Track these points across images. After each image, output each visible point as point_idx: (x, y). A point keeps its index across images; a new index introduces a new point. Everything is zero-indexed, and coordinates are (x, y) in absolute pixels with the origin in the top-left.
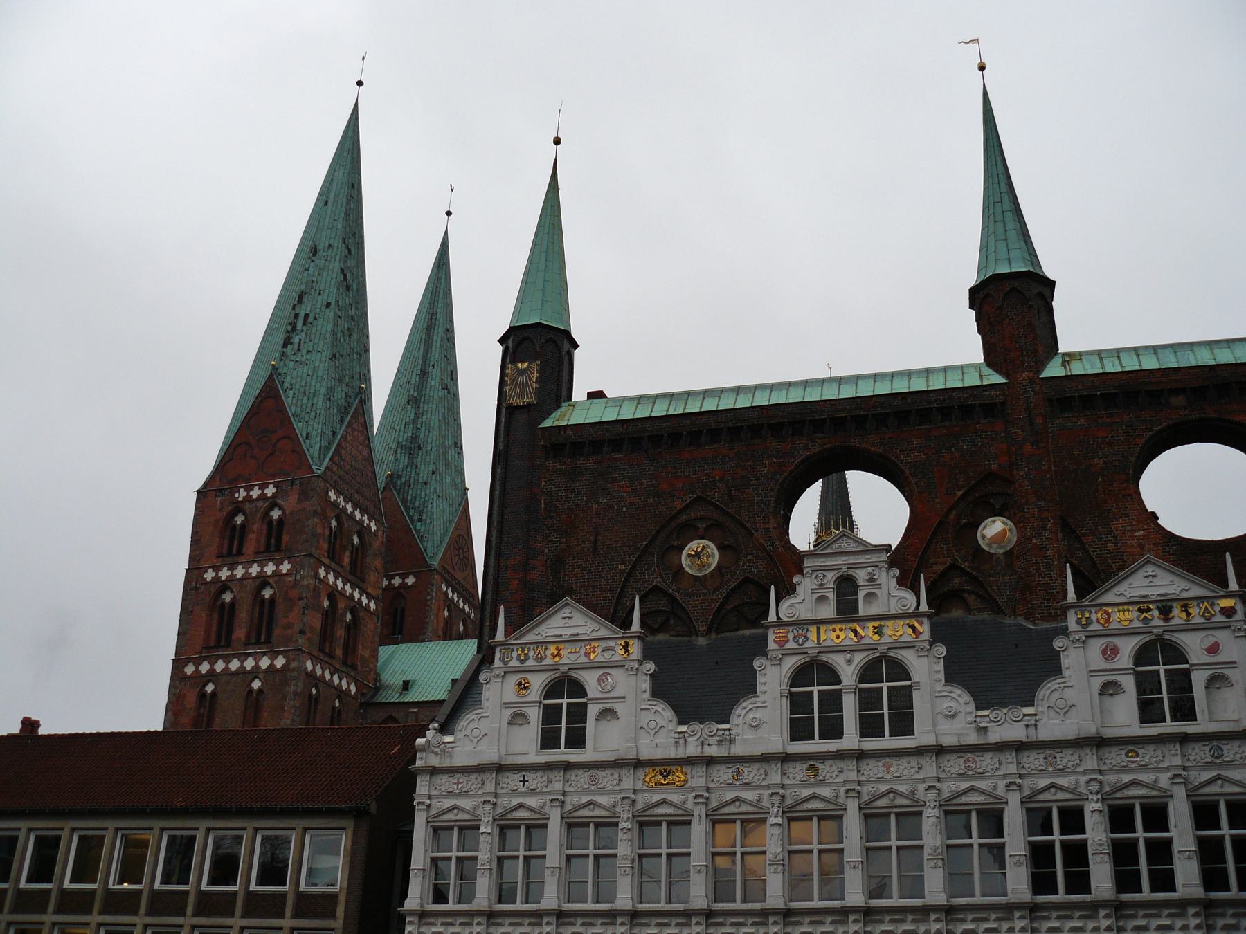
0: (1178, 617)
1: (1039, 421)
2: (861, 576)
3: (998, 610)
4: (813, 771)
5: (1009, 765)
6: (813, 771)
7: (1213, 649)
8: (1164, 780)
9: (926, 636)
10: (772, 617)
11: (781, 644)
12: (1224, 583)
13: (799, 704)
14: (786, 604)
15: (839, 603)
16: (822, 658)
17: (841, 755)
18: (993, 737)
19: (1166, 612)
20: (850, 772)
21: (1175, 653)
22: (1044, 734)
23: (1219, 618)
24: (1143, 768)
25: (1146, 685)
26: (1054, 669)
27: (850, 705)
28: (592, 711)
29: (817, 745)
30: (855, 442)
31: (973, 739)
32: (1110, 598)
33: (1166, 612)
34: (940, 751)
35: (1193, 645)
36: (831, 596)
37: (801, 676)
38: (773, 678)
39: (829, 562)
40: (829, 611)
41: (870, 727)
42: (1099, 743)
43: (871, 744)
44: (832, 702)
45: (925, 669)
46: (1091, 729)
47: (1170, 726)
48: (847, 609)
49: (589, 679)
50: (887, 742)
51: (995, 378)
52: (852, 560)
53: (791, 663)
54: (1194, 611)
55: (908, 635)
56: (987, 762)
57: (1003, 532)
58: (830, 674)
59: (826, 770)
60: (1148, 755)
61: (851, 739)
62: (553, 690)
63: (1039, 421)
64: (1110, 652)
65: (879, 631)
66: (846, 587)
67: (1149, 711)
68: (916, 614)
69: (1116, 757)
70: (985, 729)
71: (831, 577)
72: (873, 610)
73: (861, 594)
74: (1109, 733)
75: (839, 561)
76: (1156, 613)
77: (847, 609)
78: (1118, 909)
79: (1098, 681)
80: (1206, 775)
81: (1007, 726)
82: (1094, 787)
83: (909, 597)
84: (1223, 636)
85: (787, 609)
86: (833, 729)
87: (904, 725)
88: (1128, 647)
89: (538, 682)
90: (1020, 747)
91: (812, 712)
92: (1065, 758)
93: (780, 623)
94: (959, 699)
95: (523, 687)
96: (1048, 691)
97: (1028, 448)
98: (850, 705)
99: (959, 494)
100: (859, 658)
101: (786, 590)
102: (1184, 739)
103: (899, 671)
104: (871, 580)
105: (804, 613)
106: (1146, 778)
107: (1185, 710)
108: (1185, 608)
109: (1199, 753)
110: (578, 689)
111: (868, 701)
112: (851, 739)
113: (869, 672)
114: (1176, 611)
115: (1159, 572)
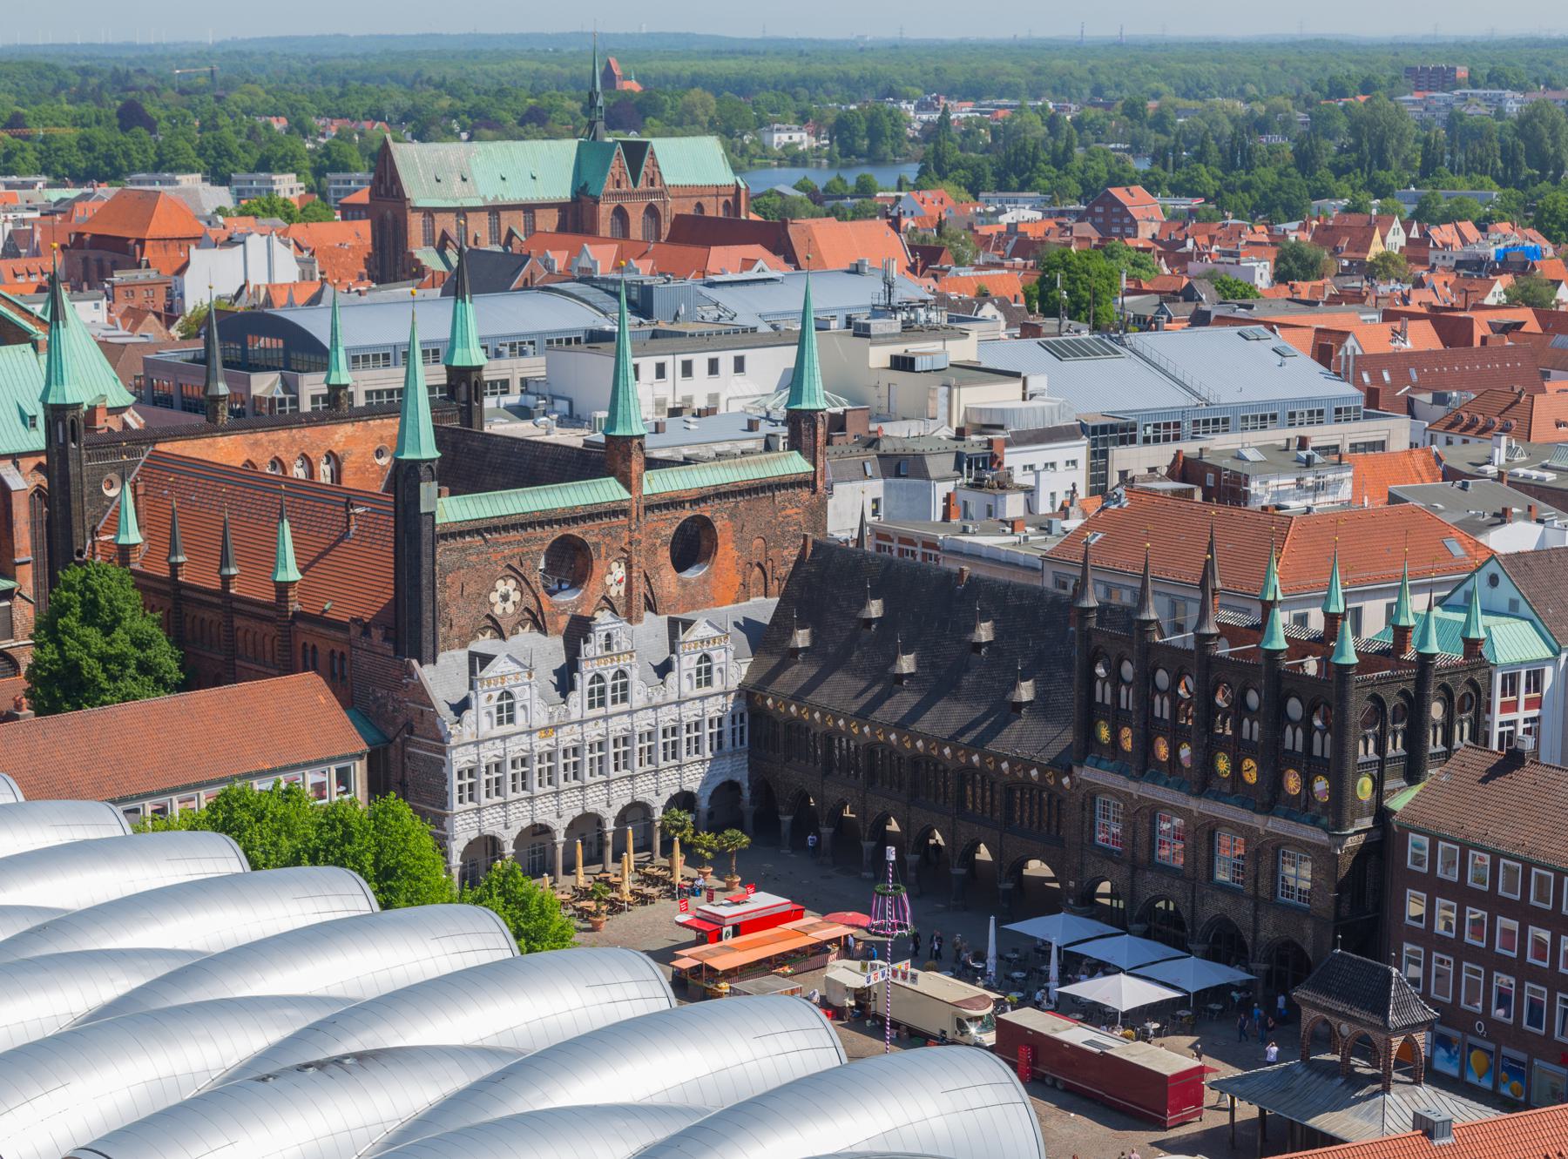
13: (591, 693)
14: (588, 646)
17: (606, 718)
27: (609, 691)
28: (518, 706)
35: (713, 654)
38: (583, 682)
44: (602, 691)
48: (608, 647)
49: (516, 691)
53: (590, 676)
58: (600, 678)
62: (500, 699)
77: (608, 647)
86: (602, 703)
87: (624, 698)
89: (496, 694)
95: (490, 697)
98: (609, 691)
110: (509, 695)
111: (614, 689)
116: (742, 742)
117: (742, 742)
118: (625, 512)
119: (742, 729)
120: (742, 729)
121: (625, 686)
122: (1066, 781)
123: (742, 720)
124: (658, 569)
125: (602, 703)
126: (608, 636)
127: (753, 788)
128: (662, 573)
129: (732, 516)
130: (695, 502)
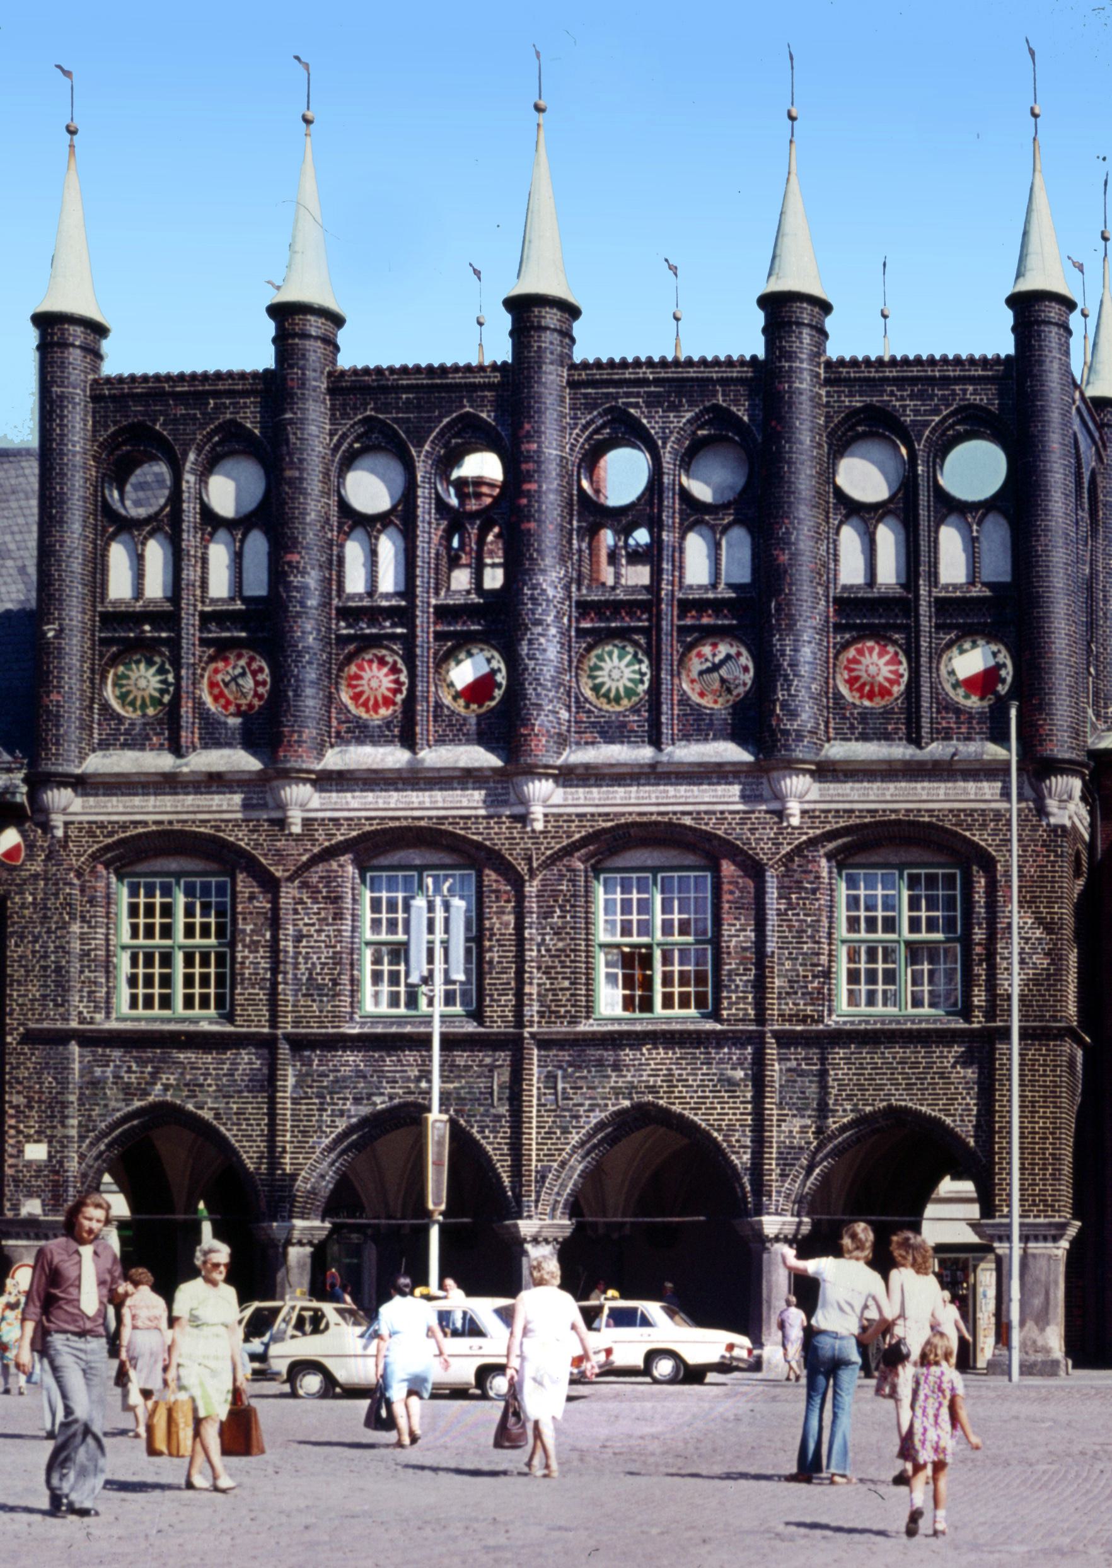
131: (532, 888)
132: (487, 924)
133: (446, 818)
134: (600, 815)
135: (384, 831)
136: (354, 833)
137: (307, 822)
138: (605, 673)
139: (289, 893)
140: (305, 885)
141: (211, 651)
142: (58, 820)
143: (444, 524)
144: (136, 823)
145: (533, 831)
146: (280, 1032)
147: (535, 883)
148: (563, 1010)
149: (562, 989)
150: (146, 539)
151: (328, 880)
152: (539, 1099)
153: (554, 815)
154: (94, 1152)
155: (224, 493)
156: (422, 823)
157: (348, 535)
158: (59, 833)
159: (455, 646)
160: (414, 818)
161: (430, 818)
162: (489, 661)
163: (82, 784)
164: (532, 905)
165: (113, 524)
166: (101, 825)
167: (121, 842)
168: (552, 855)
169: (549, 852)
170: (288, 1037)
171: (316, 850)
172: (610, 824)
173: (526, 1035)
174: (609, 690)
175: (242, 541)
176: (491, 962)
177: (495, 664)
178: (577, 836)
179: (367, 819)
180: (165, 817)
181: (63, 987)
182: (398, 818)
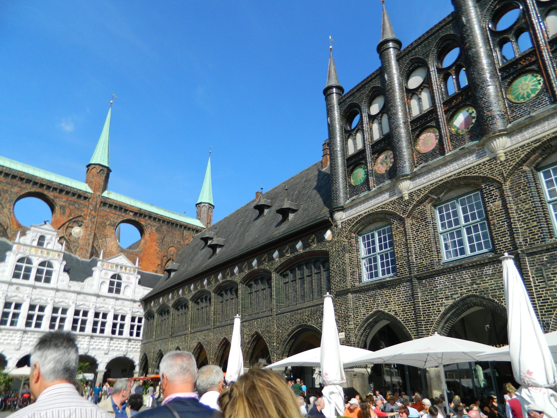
0: (123, 270)
1: (98, 206)
2: (48, 237)
3: (72, 252)
4: (17, 289)
5: (73, 296)
6: (17, 289)
7: (129, 279)
8: (110, 307)
9: (61, 258)
10: (17, 240)
11: (19, 249)
12: (135, 264)
13: (18, 268)
15: (38, 242)
16: (30, 257)
18: (72, 289)
19: (121, 268)
20: (29, 290)
21: (119, 278)
22: (85, 291)
23: (132, 272)
24: (106, 304)
25: (112, 283)
26: (90, 274)
29: (20, 281)
30: (46, 193)
31: (66, 288)
32: (110, 261)
33: (121, 268)
34: (57, 290)
35: (124, 277)
36: (37, 240)
37: (21, 260)
39: (40, 230)
40: (35, 243)
41: (38, 279)
42: (98, 296)
43: (38, 284)
44: (28, 270)
45: (58, 266)
46: (96, 292)
47: (114, 295)
50: (42, 284)
51: (90, 191)
52: (47, 232)
53: (20, 256)
54: (128, 269)
55: (56, 257)
56: (70, 294)
57: (80, 232)
58: (29, 262)
59: (22, 288)
60: (108, 300)
61: (32, 281)
63: (98, 206)
64: (106, 274)
65: (48, 253)
66: (42, 238)
67: (110, 290)
68: (61, 252)
69: (101, 299)
70: (70, 287)
71: (39, 235)
72: (50, 247)
73: (46, 242)
74: (100, 294)
75: (43, 231)
76: (119, 267)
78: (92, 337)
79: (101, 281)
80: (119, 308)
81: (76, 286)
82: (94, 306)
83: (60, 246)
84: (131, 276)
85: (23, 240)
86: (26, 277)
87: (48, 280)
88: (111, 274)
90: (79, 293)
91: (21, 271)
92: (89, 298)
93: (19, 243)
94: (66, 276)
96: (88, 280)
97: (93, 212)
99: (71, 218)
100: (41, 260)
101: (23, 234)
102: (117, 299)
103: (50, 265)
104: (51, 239)
105: (28, 242)
106: (106, 306)
107: (118, 291)
108: (126, 268)
109: (119, 302)
111: (39, 271)
112: (32, 281)
113: (42, 264)
114: (124, 268)
115: (123, 258)
116: (138, 335)
117: (138, 335)
118: (86, 198)
119: (139, 328)
120: (139, 328)
121: (49, 273)
122: (328, 235)
123: (140, 320)
124: (106, 236)
125: (26, 277)
126: (42, 238)
127: (141, 364)
128: (108, 239)
129: (158, 230)
130: (136, 214)
131: (507, 186)
132: (489, 209)
133: (461, 172)
134: (532, 142)
135: (438, 187)
136: (427, 192)
137: (411, 195)
138: (520, 89)
139: (408, 222)
140: (413, 217)
141: (376, 156)
142: (339, 223)
143: (442, 76)
144: (359, 216)
145: (501, 162)
146: (412, 275)
147: (507, 184)
148: (536, 236)
149: (533, 227)
150: (356, 134)
151: (422, 213)
152: (535, 283)
153: (509, 151)
154: (360, 333)
155: (375, 109)
156: (452, 178)
157: (411, 99)
158: (340, 227)
159: (452, 112)
160: (448, 177)
161: (455, 175)
162: (468, 111)
163: (342, 209)
164: (508, 193)
165: (348, 134)
166: (350, 220)
167: (357, 223)
168: (512, 168)
169: (510, 168)
170: (415, 277)
171: (414, 203)
172: (538, 144)
173: (520, 252)
174: (524, 94)
175: (381, 120)
176: (494, 224)
177: (470, 111)
178: (523, 156)
179: (431, 185)
180: (367, 210)
181: (345, 276)
182: (442, 180)
